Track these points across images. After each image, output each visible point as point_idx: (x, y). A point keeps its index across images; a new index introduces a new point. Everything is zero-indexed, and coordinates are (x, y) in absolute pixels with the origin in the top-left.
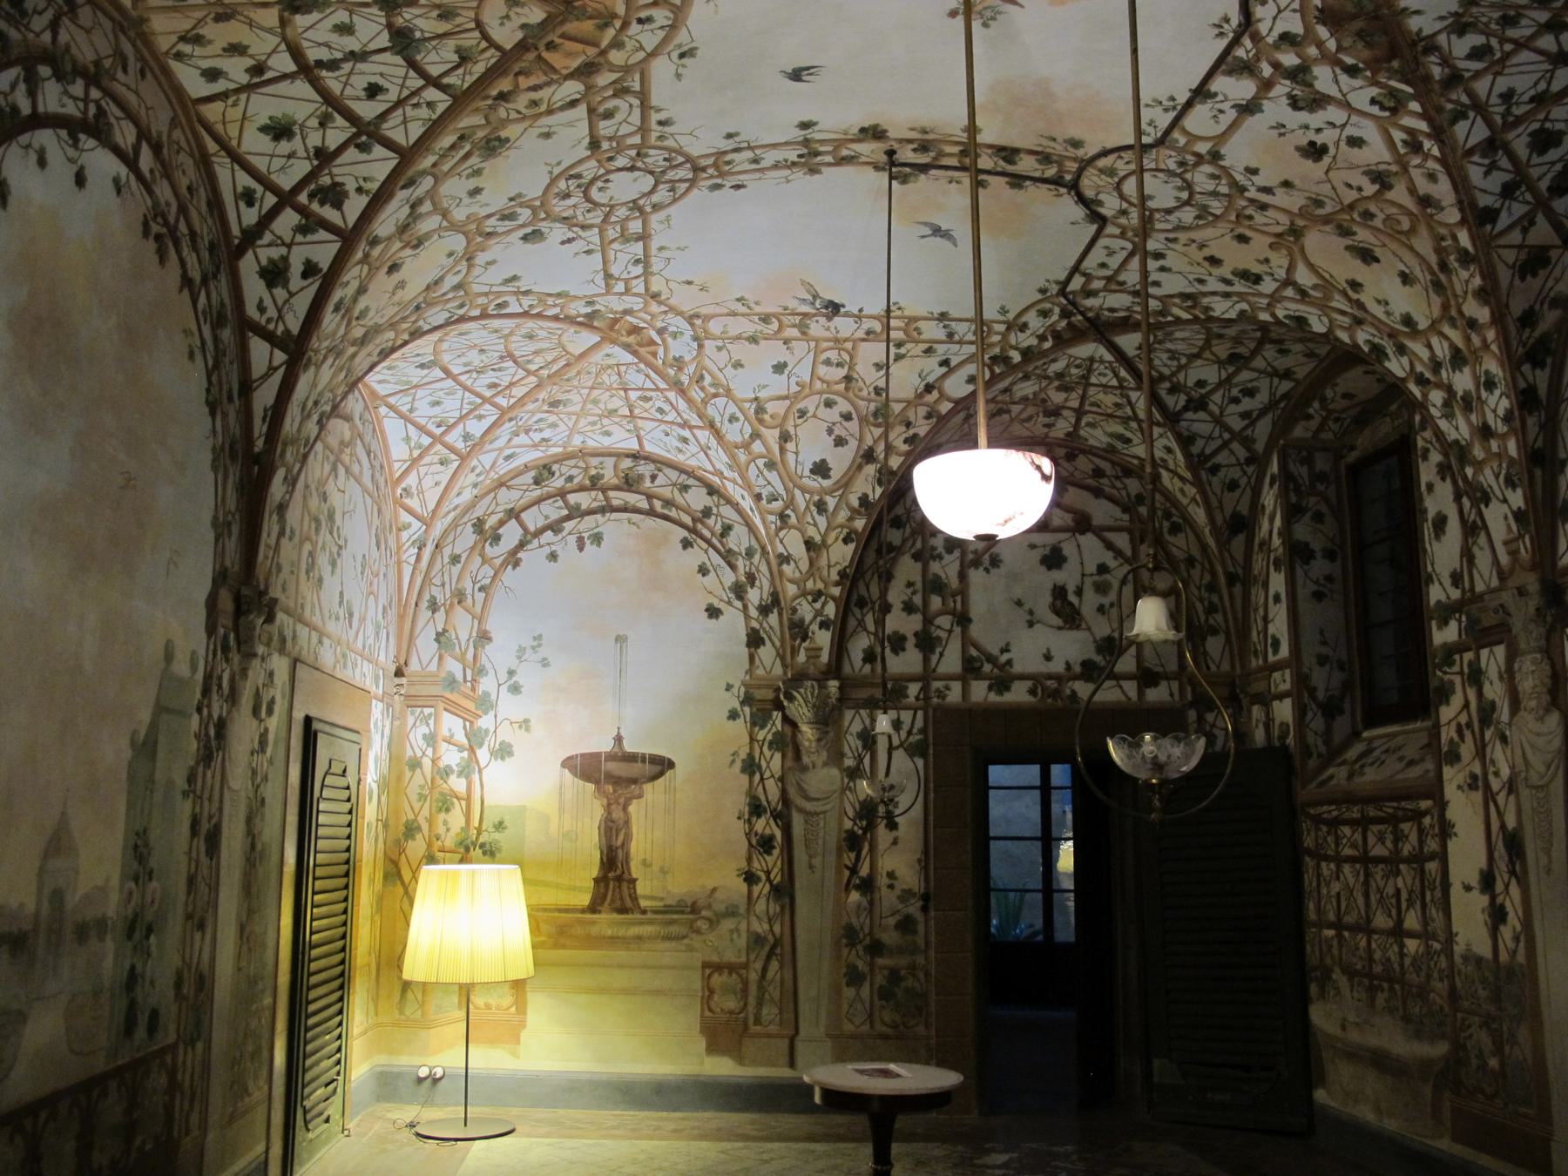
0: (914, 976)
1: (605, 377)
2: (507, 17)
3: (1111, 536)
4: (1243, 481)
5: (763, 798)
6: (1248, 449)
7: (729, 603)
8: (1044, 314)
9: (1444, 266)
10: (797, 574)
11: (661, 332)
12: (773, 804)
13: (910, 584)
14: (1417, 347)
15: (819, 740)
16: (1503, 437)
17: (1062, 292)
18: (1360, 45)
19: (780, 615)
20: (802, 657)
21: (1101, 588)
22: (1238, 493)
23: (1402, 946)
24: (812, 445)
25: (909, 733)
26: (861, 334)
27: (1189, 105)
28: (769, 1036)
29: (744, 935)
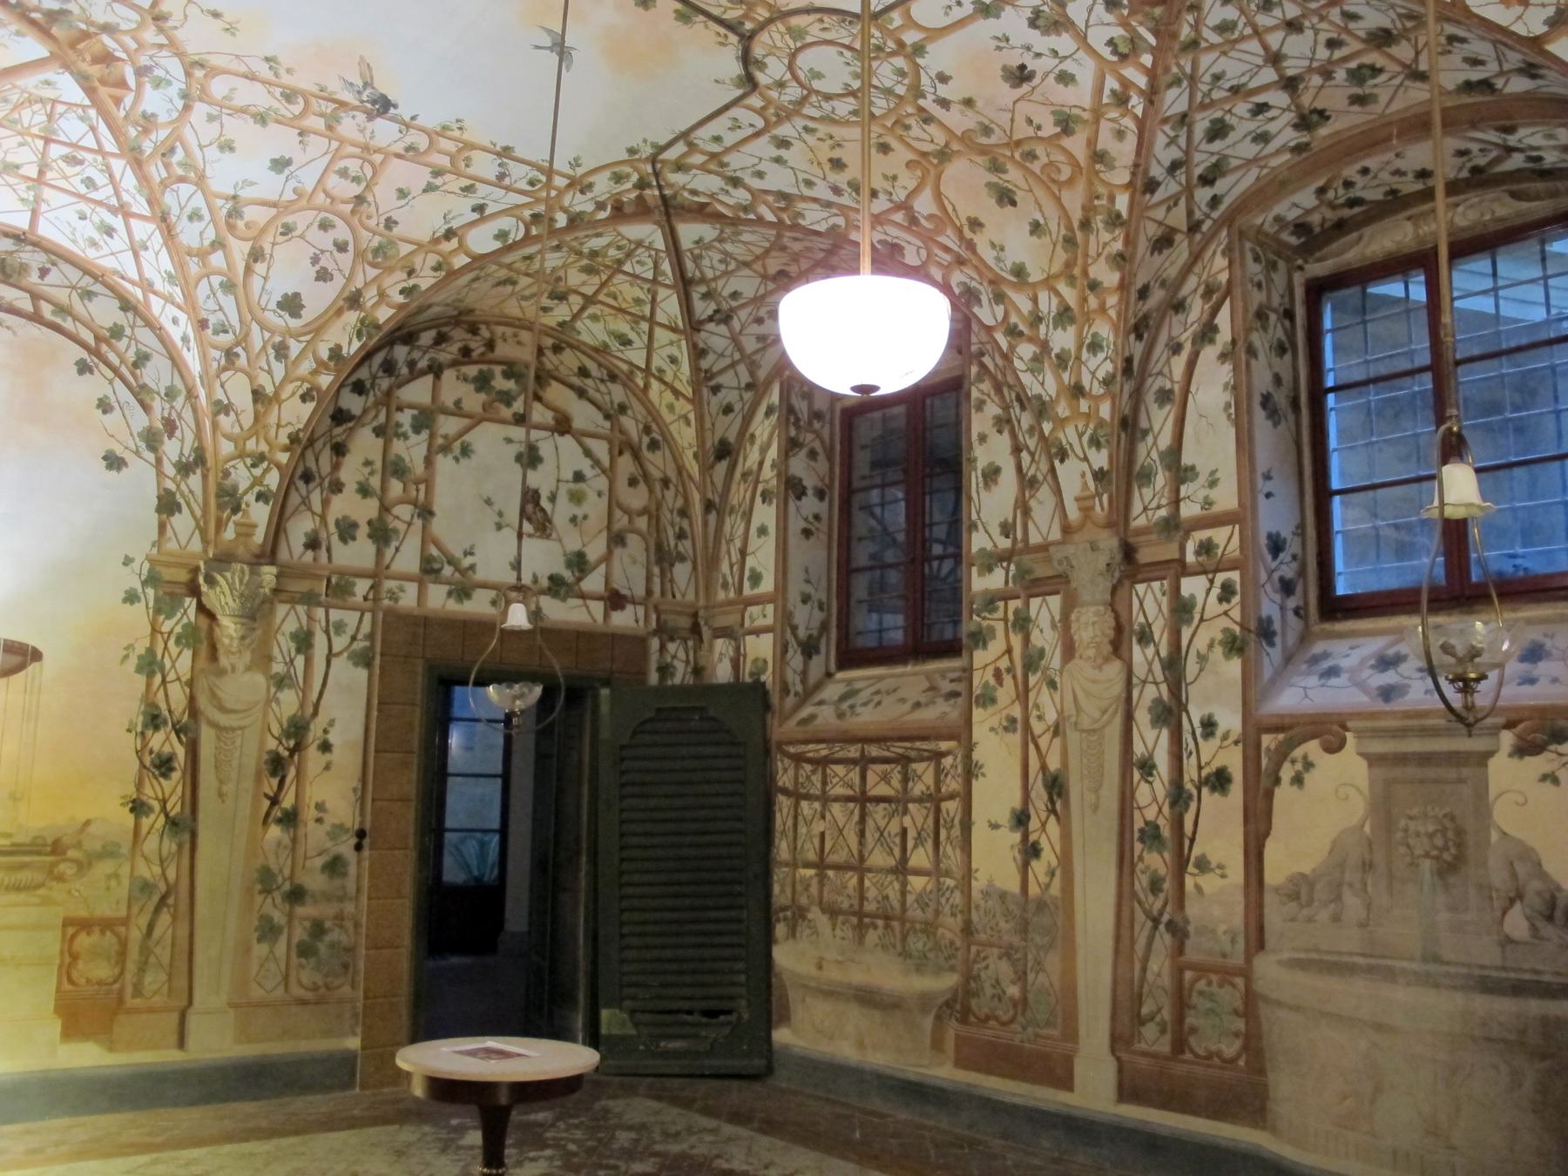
0: (341, 927)
1: (26, 114)
3: (589, 442)
4: (737, 407)
5: (163, 706)
6: (752, 374)
7: (137, 453)
8: (618, 178)
9: (1086, 224)
10: (237, 430)
11: (141, 72)
12: (177, 714)
13: (367, 463)
14: (1023, 302)
15: (243, 638)
16: (1098, 399)
17: (653, 160)
19: (205, 477)
20: (229, 533)
21: (576, 498)
22: (731, 416)
23: (904, 884)
24: (288, 271)
25: (354, 638)
26: (399, 148)
28: (151, 1010)
29: (126, 882)
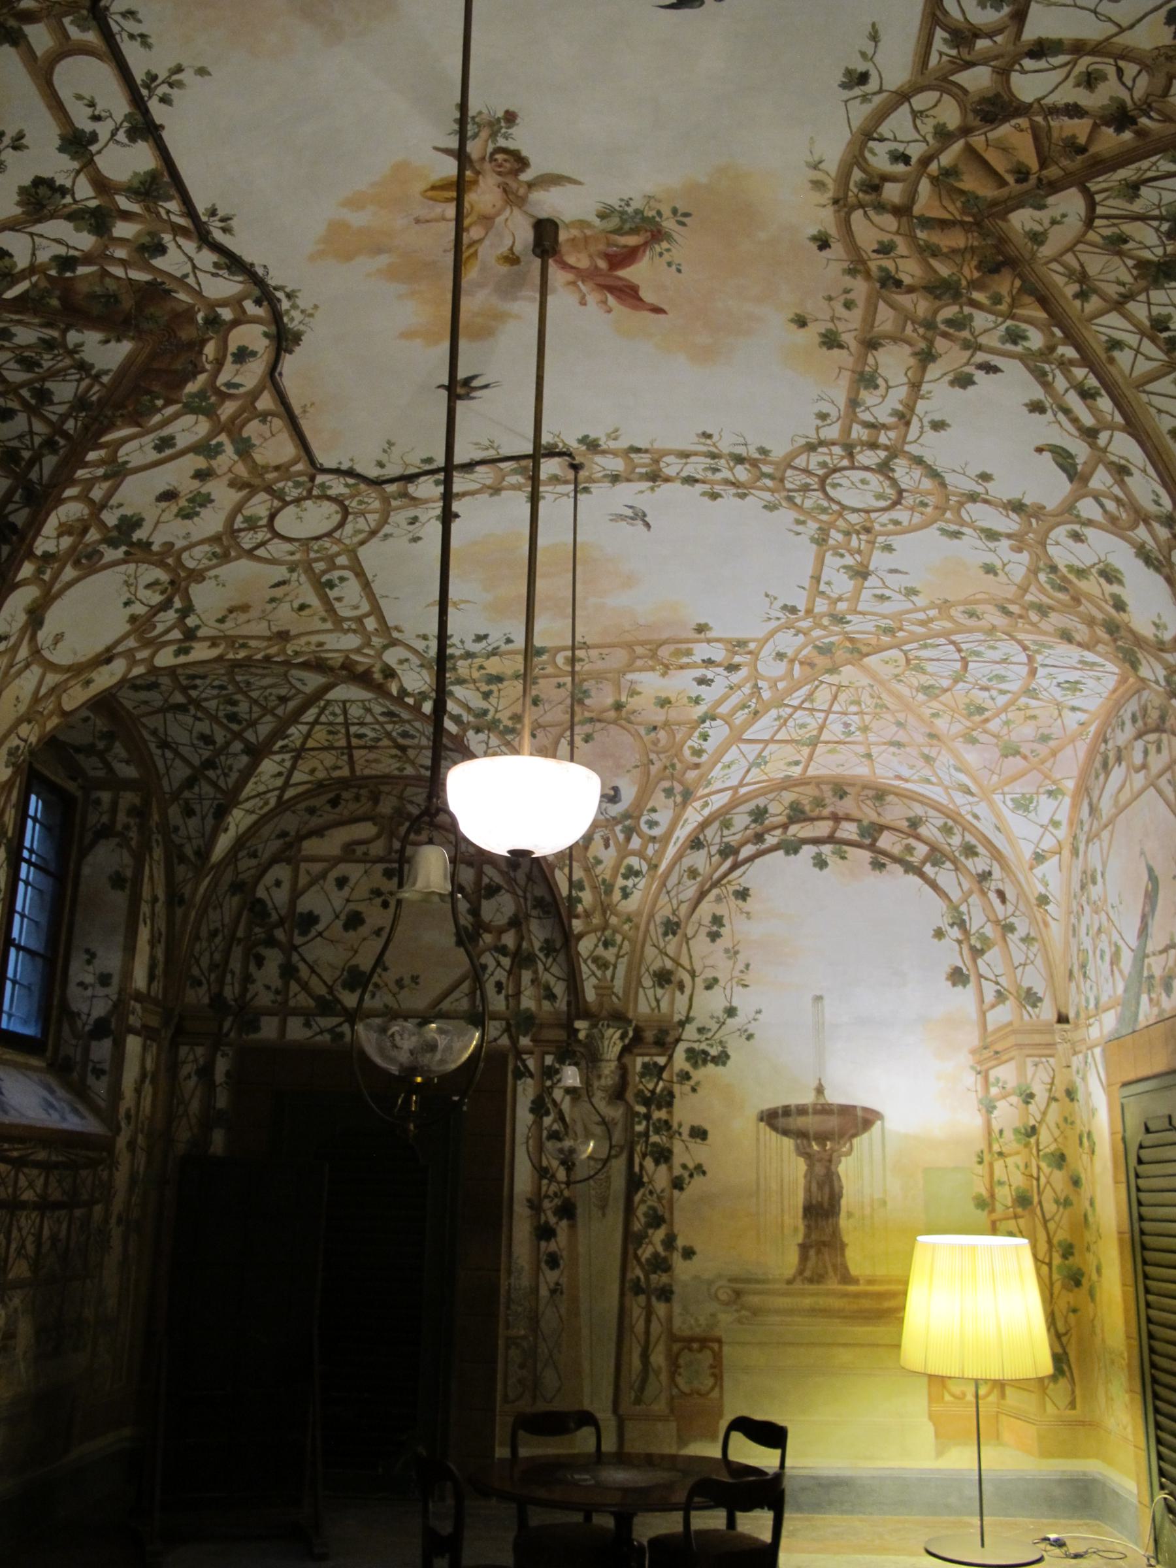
2: (1054, 222)
18: (98, 289)
27: (138, 102)
